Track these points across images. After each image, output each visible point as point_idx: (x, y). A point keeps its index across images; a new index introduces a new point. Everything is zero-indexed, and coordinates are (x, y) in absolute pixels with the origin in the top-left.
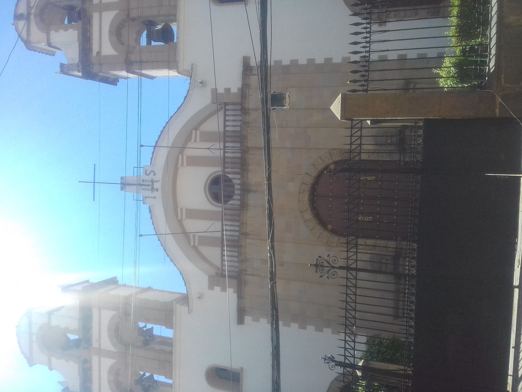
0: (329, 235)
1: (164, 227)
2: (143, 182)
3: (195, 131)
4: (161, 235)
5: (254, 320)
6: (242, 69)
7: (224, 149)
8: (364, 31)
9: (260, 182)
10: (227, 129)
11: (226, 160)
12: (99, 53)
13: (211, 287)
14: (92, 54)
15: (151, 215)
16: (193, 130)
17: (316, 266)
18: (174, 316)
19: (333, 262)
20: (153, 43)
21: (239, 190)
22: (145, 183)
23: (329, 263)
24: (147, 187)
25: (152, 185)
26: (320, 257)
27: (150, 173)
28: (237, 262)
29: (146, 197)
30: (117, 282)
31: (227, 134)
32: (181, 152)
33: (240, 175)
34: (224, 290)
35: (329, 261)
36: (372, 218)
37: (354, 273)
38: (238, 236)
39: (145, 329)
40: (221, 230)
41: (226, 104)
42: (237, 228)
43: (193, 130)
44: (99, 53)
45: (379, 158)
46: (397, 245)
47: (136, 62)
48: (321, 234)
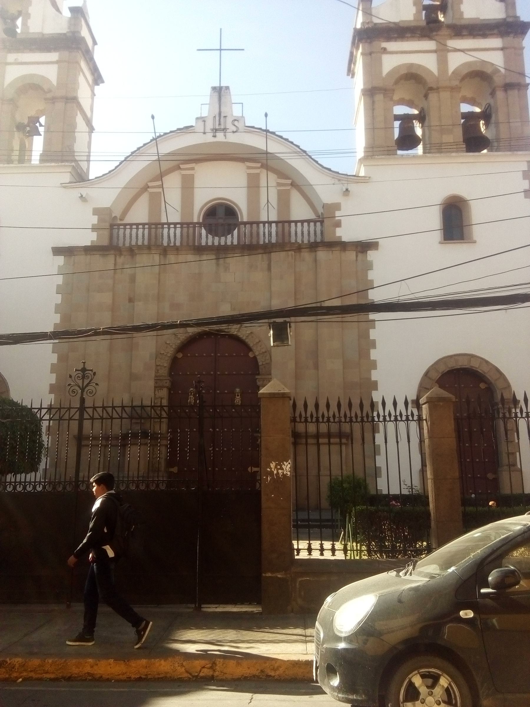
0: (169, 355)
1: (166, 148)
2: (225, 117)
3: (290, 183)
4: (155, 144)
8: (364, 414)
9: (229, 269)
12: (385, 51)
13: (96, 211)
14: (383, 42)
16: (291, 181)
17: (84, 370)
18: (56, 164)
19: (88, 391)
20: (397, 124)
21: (219, 243)
22: (222, 119)
23: (87, 385)
24: (217, 123)
26: (95, 374)
29: (204, 121)
30: (98, 84)
31: (286, 225)
32: (262, 166)
34: (94, 229)
35: (91, 384)
36: (193, 404)
37: (77, 416)
39: (38, 124)
41: (322, 222)
43: (291, 181)
44: (385, 51)
47: (373, 102)
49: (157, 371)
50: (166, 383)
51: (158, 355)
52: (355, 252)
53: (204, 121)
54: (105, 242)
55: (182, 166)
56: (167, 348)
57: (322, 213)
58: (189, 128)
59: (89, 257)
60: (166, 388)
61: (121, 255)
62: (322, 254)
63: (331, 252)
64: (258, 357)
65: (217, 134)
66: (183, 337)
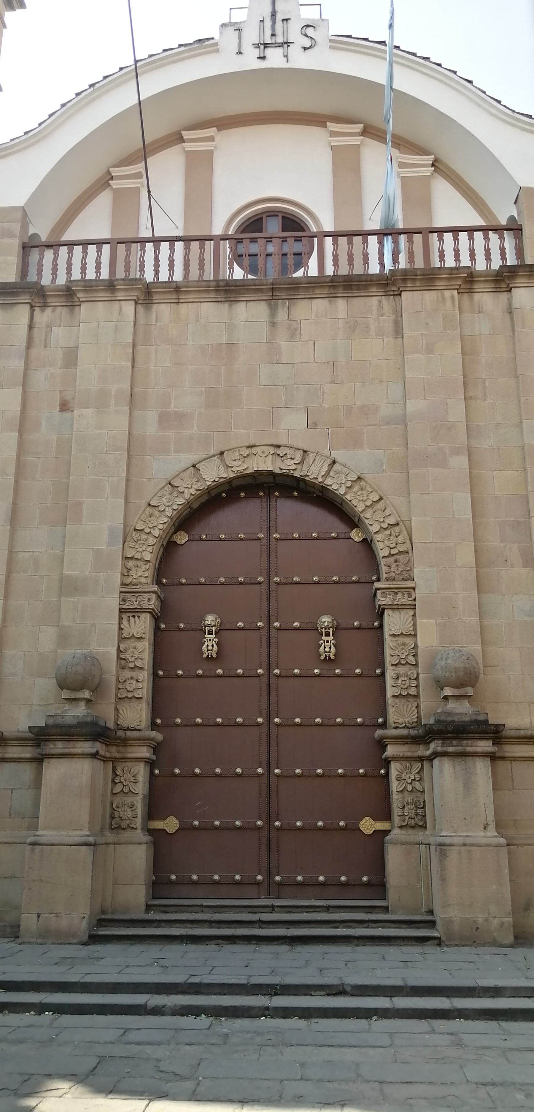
0: (156, 533)
2: (283, 20)
3: (431, 162)
9: (301, 334)
10: (448, 237)
11: (357, 240)
15: (190, 44)
22: (279, 25)
24: (268, 32)
25: (276, 43)
27: (306, 35)
28: (69, 281)
29: (239, 30)
40: (155, 236)
43: (433, 156)
45: (392, 665)
48: (160, 511)
49: (126, 572)
50: (149, 600)
53: (239, 30)
55: (186, 135)
58: (204, 42)
60: (148, 615)
61: (44, 306)
64: (378, 537)
65: (270, 52)
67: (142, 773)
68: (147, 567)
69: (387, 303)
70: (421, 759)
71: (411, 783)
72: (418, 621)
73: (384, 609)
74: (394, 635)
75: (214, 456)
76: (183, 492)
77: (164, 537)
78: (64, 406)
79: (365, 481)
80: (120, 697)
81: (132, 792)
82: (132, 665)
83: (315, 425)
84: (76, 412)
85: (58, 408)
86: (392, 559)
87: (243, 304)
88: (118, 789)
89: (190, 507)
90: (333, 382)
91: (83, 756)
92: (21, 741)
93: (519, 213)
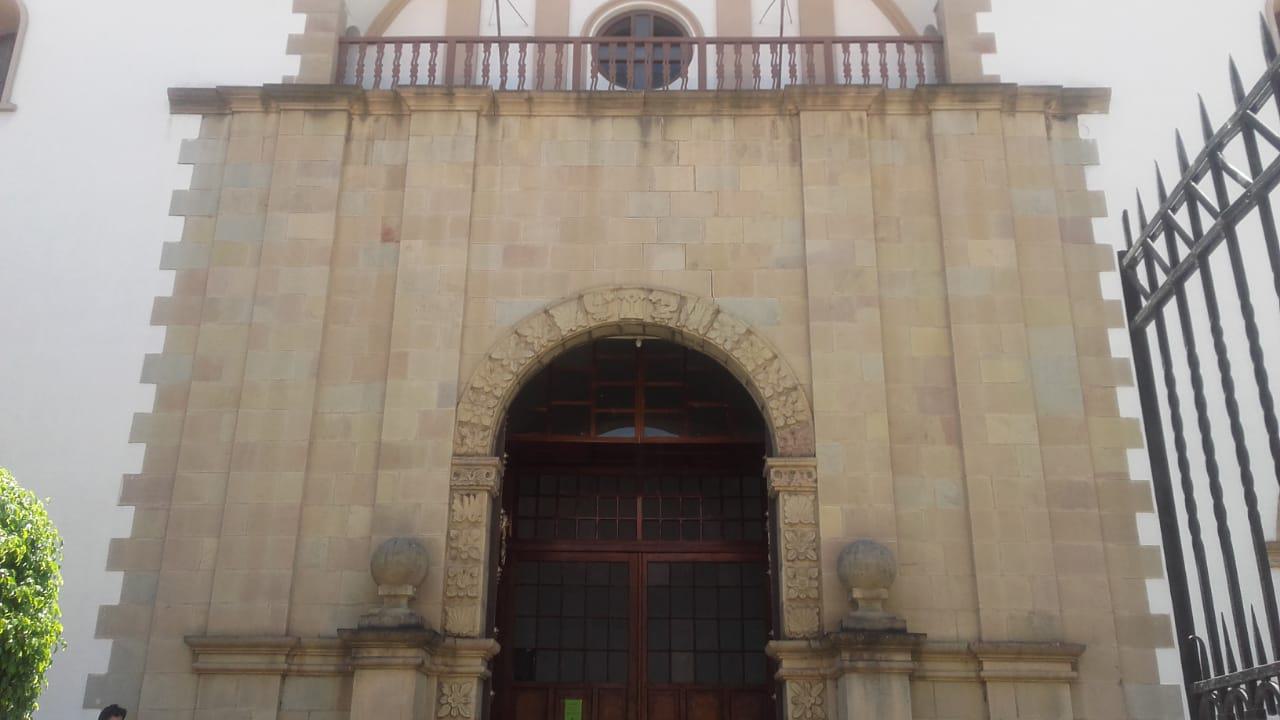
0: (498, 393)
5: (186, 145)
6: (1066, 85)
7: (781, 41)
9: (678, 158)
10: (855, 48)
11: (746, 49)
33: (696, 87)
34: (295, 45)
38: (485, 86)
40: (502, 34)
42: (512, 83)
45: (788, 561)
46: (473, 638)
48: (502, 366)
51: (464, 393)
52: (1043, 116)
54: (324, 75)
56: (492, 371)
57: (930, 28)
59: (273, 117)
61: (365, 115)
62: (948, 120)
63: (974, 115)
64: (772, 404)
66: (544, 342)
67: (475, 687)
68: (486, 433)
69: (782, 125)
70: (824, 678)
71: (811, 708)
72: (822, 507)
73: (779, 492)
74: (791, 524)
75: (571, 300)
76: (533, 343)
77: (507, 397)
78: (388, 236)
79: (757, 336)
80: (449, 594)
81: (462, 716)
82: (464, 556)
83: (695, 266)
84: (401, 243)
85: (379, 238)
86: (788, 430)
87: (610, 119)
88: (444, 712)
89: (539, 362)
90: (716, 215)
91: (405, 666)
92: (324, 647)
93: (940, 22)
